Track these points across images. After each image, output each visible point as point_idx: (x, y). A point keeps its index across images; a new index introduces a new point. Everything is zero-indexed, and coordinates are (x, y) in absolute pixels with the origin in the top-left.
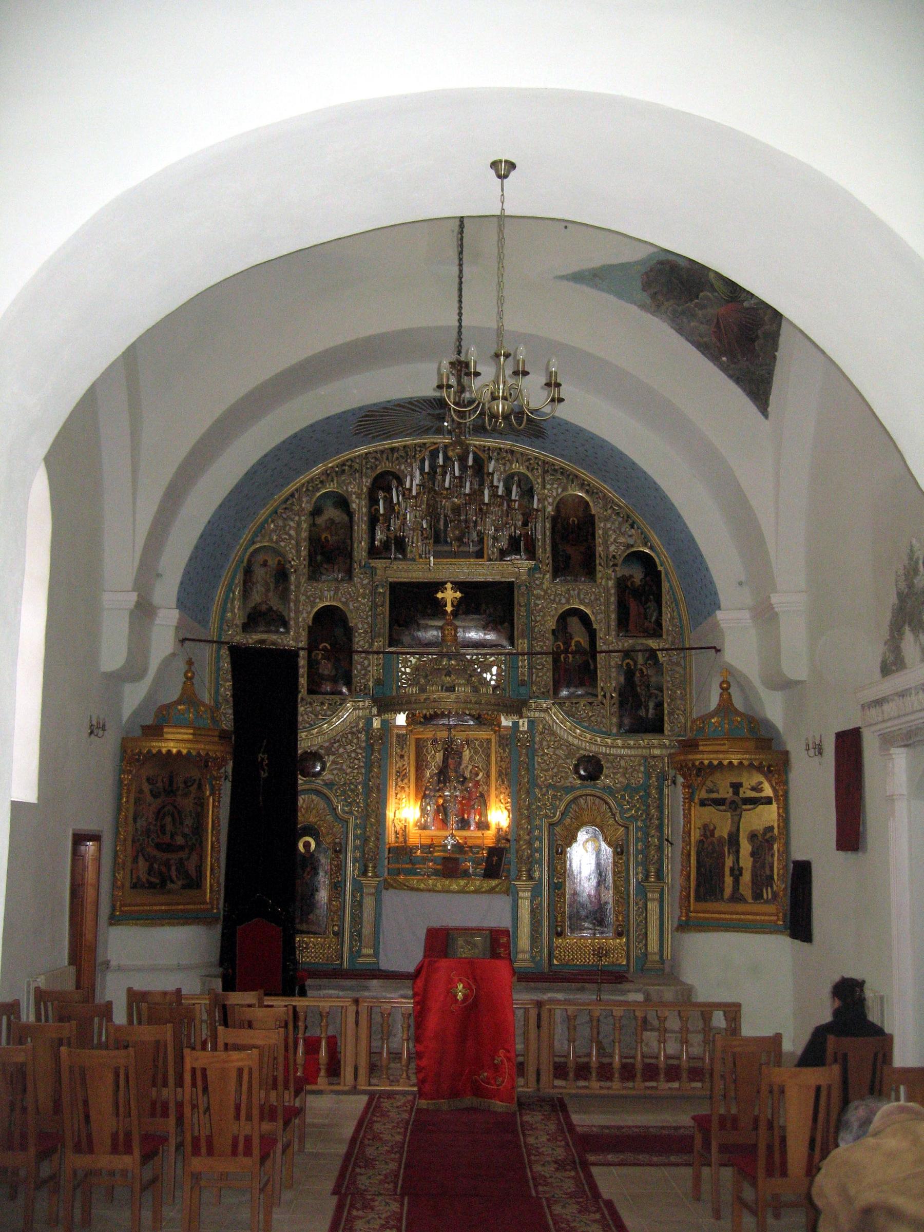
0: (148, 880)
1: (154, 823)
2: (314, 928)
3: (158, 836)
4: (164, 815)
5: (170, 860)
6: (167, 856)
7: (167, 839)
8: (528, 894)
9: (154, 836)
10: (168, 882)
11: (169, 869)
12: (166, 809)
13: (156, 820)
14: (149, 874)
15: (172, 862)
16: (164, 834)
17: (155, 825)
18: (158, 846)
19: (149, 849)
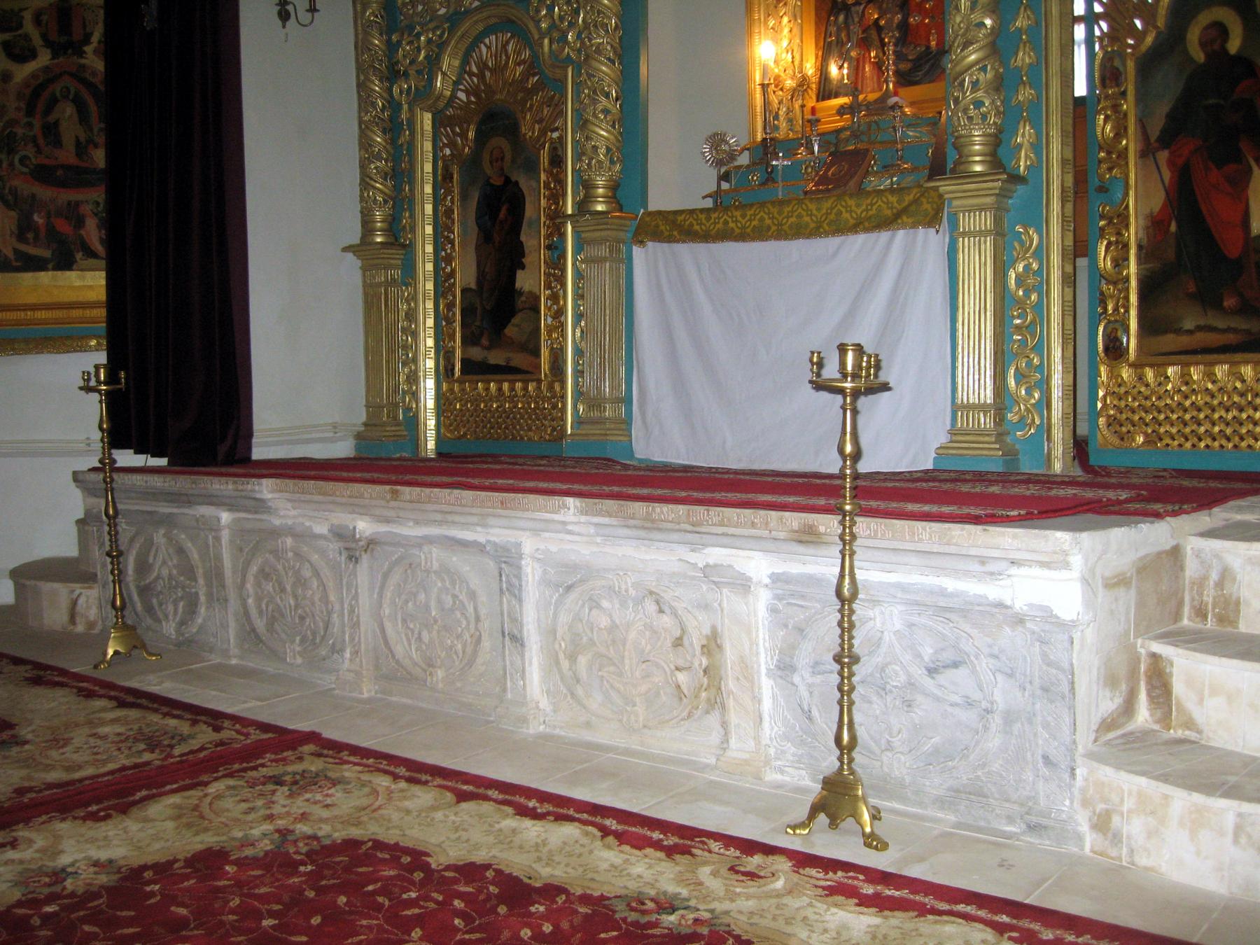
0: (16, 251)
1: (26, 120)
2: (518, 360)
3: (39, 151)
4: (54, 102)
5: (77, 204)
6: (66, 196)
7: (67, 155)
8: (985, 221)
9: (29, 151)
10: (79, 256)
11: (80, 222)
12: (57, 88)
13: (30, 112)
14: (21, 237)
15: (86, 209)
16: (58, 143)
17: (30, 125)
18: (44, 174)
19: (16, 183)
